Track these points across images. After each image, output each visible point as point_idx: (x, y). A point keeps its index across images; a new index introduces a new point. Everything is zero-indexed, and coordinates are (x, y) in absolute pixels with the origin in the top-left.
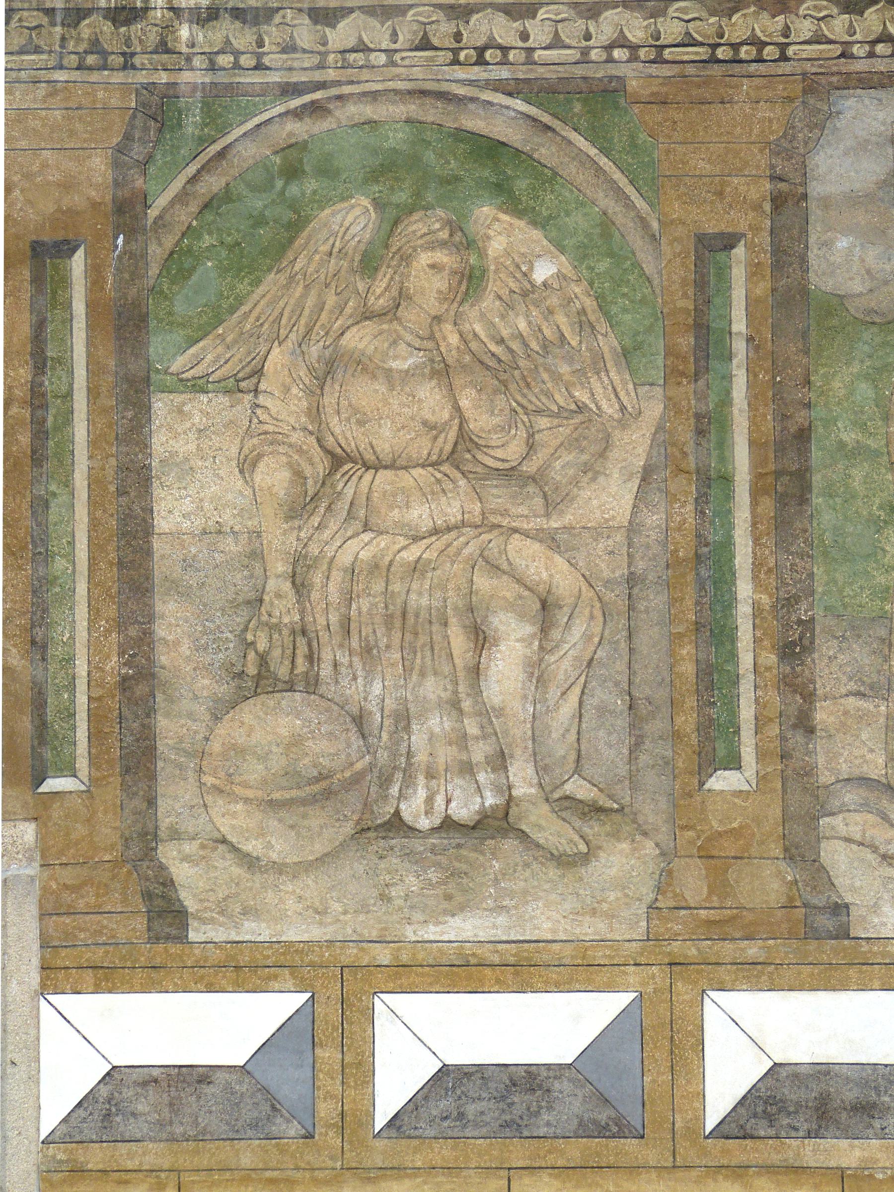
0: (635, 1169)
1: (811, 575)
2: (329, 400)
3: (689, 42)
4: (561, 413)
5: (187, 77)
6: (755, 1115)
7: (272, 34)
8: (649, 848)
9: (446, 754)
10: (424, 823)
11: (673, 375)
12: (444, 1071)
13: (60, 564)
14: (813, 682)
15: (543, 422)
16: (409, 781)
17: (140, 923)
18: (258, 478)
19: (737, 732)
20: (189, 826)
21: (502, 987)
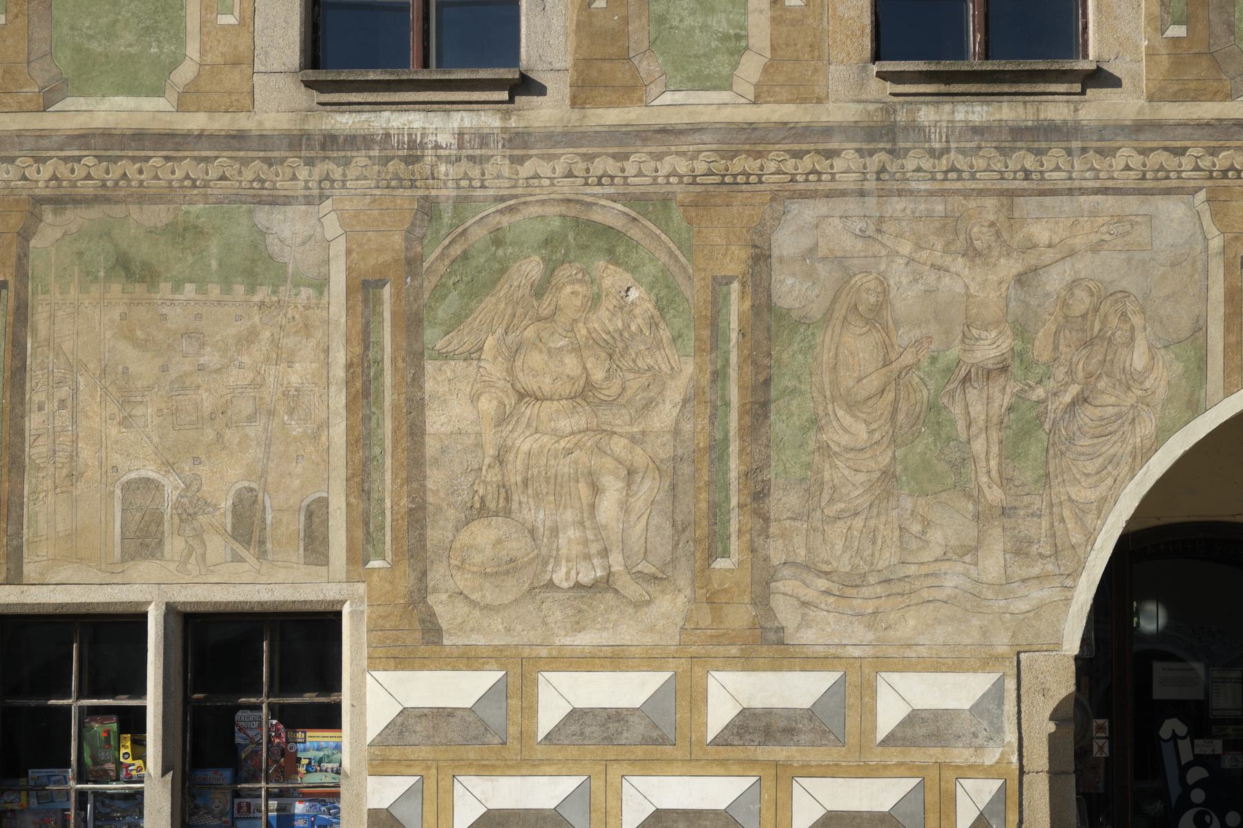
0: (670, 761)
1: (769, 457)
2: (518, 363)
3: (710, 173)
5: (444, 192)
6: (733, 734)
7: (490, 168)
8: (681, 599)
9: (576, 549)
10: (565, 585)
11: (699, 350)
12: (574, 711)
14: (768, 512)
17: (418, 635)
19: (729, 538)
21: (602, 669)
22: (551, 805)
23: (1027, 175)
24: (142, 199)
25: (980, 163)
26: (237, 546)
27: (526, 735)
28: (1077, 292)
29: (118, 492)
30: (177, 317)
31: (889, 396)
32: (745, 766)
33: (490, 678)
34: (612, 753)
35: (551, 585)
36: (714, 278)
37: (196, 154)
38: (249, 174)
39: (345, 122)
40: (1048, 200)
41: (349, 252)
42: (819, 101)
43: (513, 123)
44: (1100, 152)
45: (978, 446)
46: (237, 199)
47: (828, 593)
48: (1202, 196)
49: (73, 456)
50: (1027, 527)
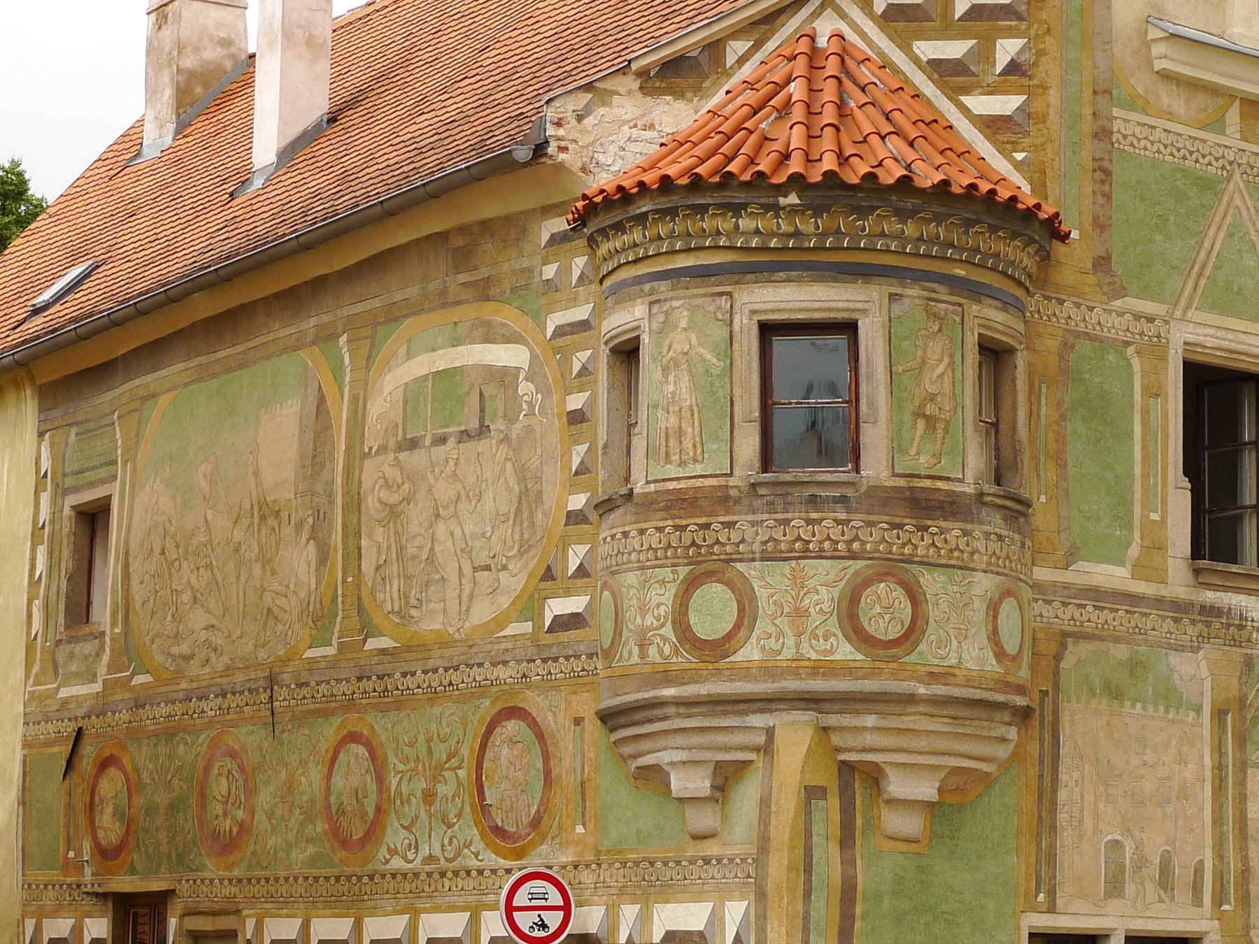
24: (1117, 640)
37: (1140, 610)
39: (1210, 597)
49: (1081, 821)
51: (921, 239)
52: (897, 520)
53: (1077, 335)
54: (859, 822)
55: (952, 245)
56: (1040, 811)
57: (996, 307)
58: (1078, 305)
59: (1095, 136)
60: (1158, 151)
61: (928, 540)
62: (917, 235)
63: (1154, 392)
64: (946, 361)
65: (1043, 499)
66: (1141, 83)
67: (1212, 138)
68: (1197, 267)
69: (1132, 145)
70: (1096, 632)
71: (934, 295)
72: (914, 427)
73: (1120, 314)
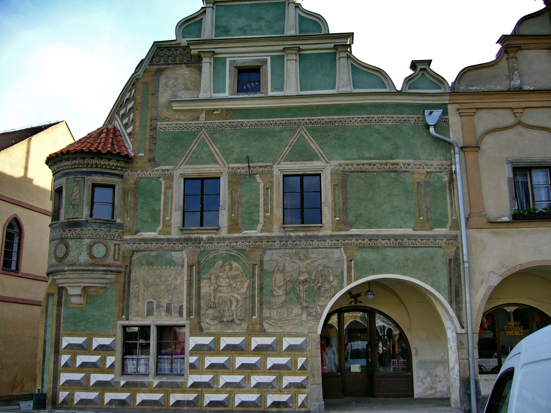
2: (217, 280)
4: (240, 281)
7: (213, 245)
8: (247, 324)
11: (250, 278)
13: (192, 296)
15: (238, 282)
16: (224, 317)
18: (211, 288)
20: (204, 321)
22: (223, 362)
23: (310, 245)
24: (152, 251)
25: (301, 243)
26: (167, 314)
27: (218, 349)
28: (320, 266)
29: (146, 304)
30: (157, 272)
31: (285, 286)
32: (259, 355)
33: (211, 338)
34: (234, 352)
35: (223, 321)
36: (253, 264)
38: (170, 246)
40: (314, 250)
41: (188, 260)
42: (272, 232)
43: (217, 236)
44: (323, 241)
45: (302, 295)
46: (167, 250)
47: (274, 323)
48: (342, 248)
50: (310, 310)
51: (72, 165)
52: (65, 229)
53: (141, 178)
54: (63, 301)
55: (80, 164)
56: (124, 295)
57: (98, 176)
58: (142, 171)
59: (151, 130)
60: (174, 129)
61: (71, 233)
62: (71, 164)
63: (169, 187)
64: (78, 191)
65: (128, 219)
66: (167, 114)
67: (194, 122)
68: (186, 155)
69: (164, 130)
70: (145, 249)
71: (76, 177)
72: (70, 207)
73: (157, 171)
